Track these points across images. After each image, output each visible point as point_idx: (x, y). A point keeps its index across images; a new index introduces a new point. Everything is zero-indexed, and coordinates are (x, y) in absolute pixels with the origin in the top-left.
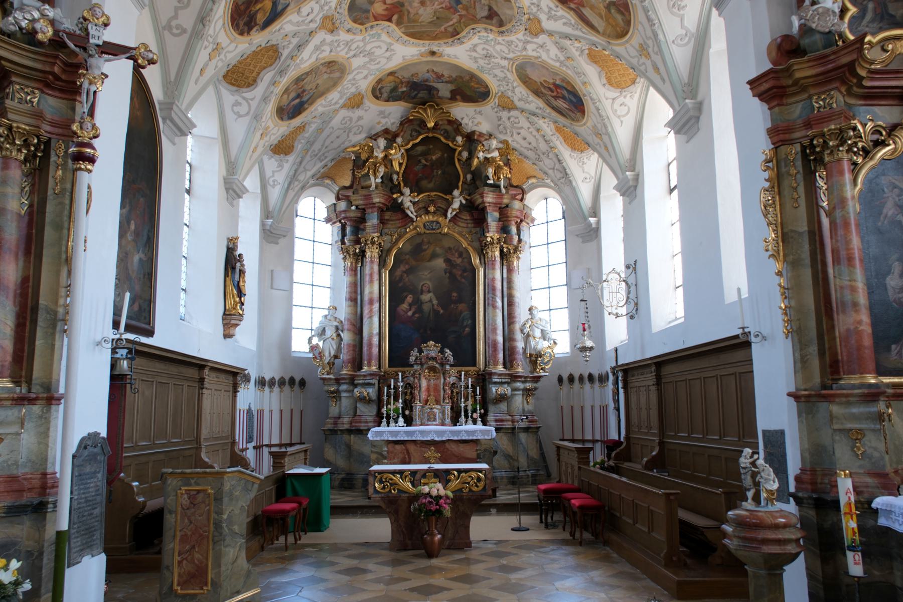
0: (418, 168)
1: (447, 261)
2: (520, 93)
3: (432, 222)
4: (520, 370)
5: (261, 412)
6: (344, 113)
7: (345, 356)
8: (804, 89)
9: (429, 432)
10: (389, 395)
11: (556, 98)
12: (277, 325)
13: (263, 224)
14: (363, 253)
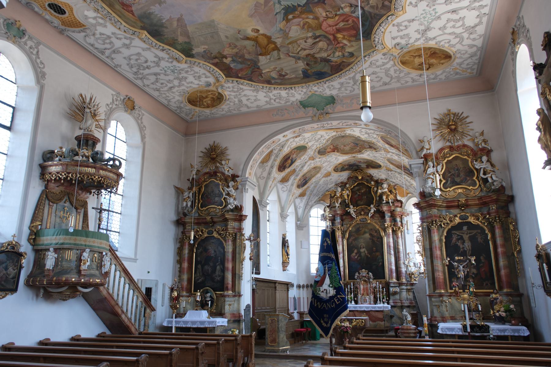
0: (356, 196)
1: (371, 234)
2: (392, 167)
4: (404, 281)
5: (299, 298)
6: (324, 179)
8: (425, 208)
9: (363, 307)
10: (348, 291)
12: (304, 263)
13: (296, 224)
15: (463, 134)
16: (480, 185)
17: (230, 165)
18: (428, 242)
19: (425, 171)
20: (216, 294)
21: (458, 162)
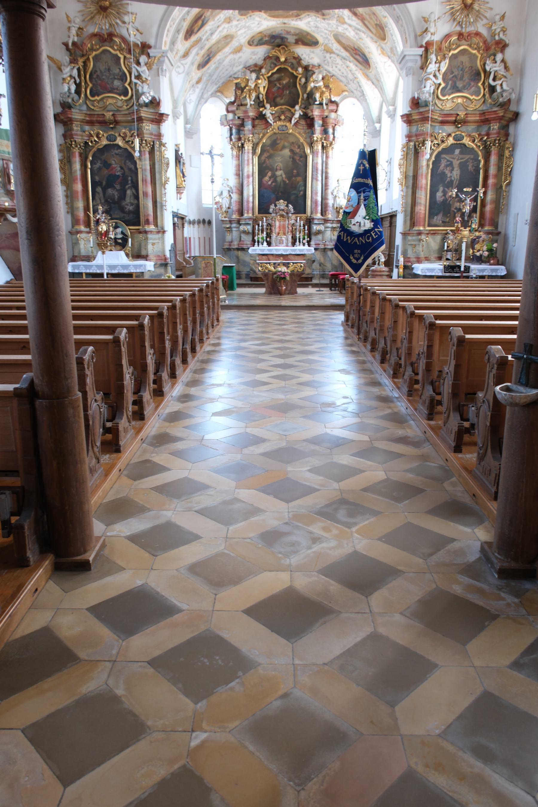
0: (274, 90)
1: (291, 151)
2: (336, 46)
3: (283, 126)
4: (330, 216)
6: (232, 56)
7: (235, 207)
8: (416, 122)
10: (258, 230)
11: (356, 54)
13: (185, 128)
14: (243, 145)
15: (479, 15)
16: (484, 95)
17: (137, 24)
18: (411, 168)
19: (423, 67)
20: (129, 229)
21: (464, 59)
